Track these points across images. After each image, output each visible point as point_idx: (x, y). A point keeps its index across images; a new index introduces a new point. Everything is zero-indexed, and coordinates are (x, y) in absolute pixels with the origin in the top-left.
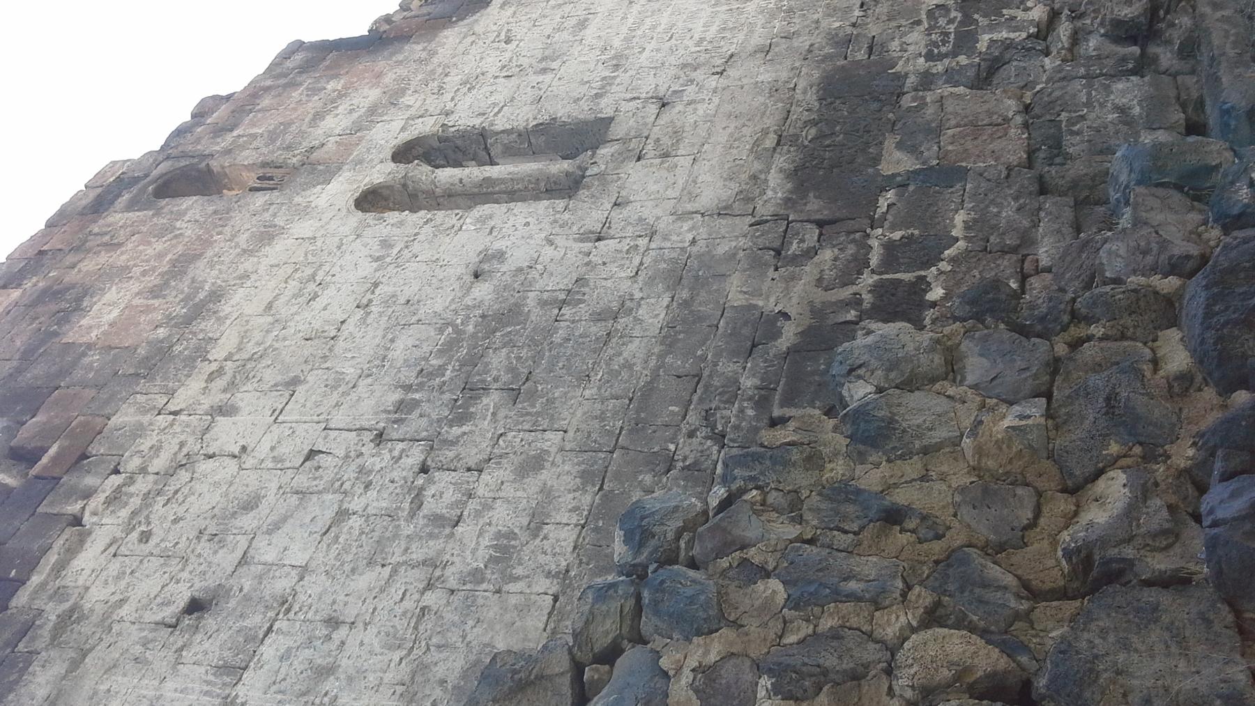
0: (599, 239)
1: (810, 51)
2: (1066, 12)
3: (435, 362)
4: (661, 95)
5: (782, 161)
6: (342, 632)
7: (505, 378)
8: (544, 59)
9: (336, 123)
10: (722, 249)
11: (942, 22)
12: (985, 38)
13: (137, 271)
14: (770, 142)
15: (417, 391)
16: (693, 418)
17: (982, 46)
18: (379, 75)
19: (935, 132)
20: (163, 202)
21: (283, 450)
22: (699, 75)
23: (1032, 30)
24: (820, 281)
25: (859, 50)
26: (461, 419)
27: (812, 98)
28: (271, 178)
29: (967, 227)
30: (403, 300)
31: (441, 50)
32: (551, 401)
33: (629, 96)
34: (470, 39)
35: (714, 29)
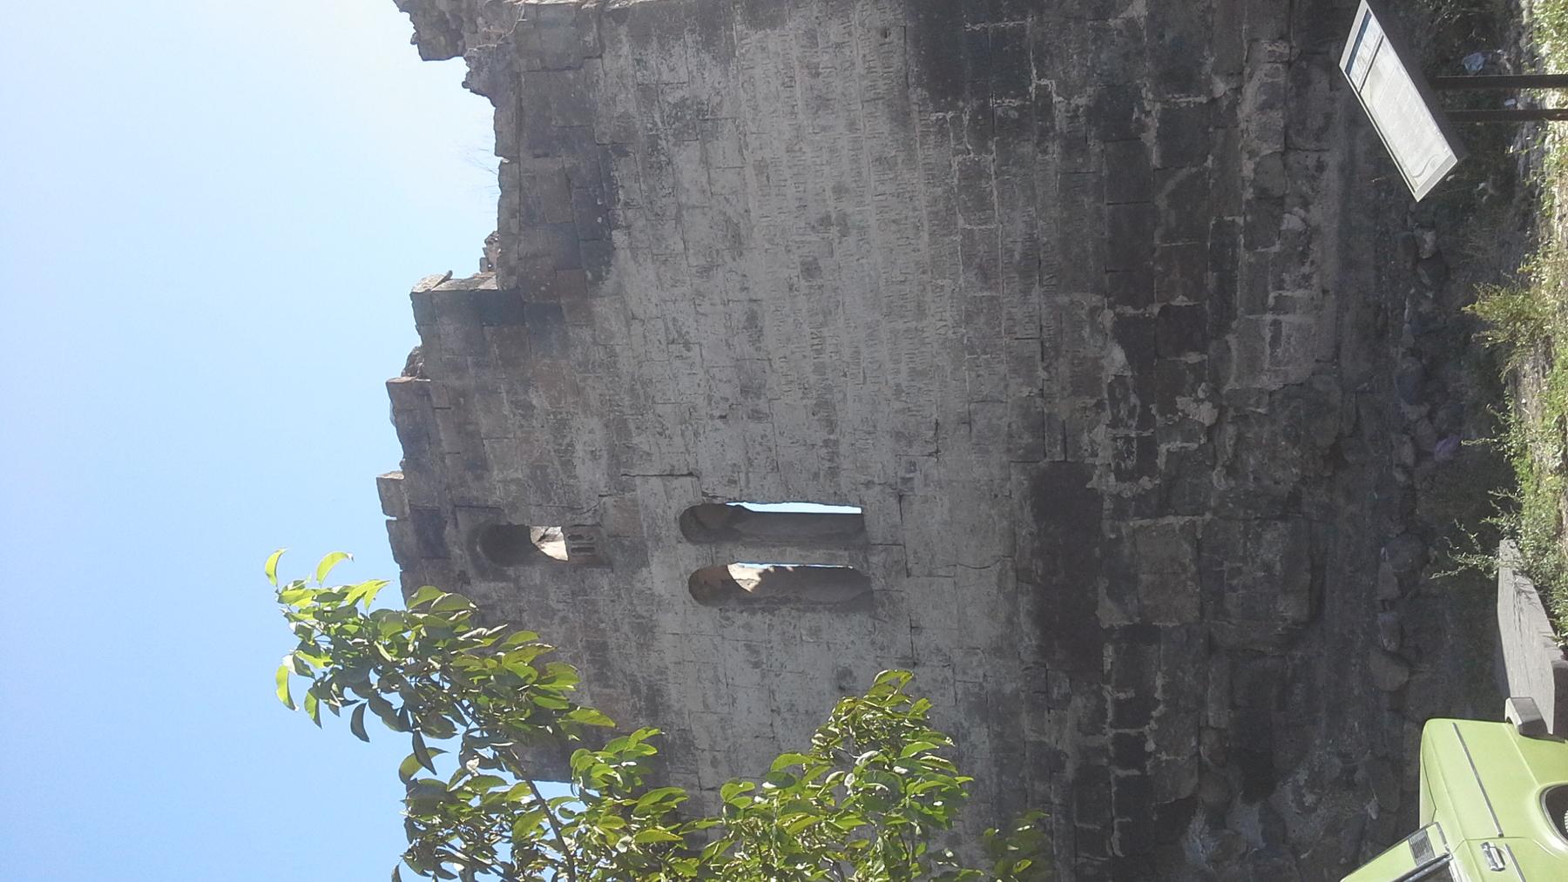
1: (1010, 436)
2: (1231, 412)
4: (892, 481)
5: (1025, 603)
8: (745, 391)
9: (590, 475)
10: (1008, 688)
12: (1163, 448)
17: (1161, 462)
18: (578, 391)
20: (511, 571)
22: (915, 451)
24: (1079, 724)
27: (1027, 514)
28: (580, 537)
29: (1164, 691)
30: (802, 710)
31: (618, 349)
33: (863, 478)
34: (636, 327)
35: (904, 368)
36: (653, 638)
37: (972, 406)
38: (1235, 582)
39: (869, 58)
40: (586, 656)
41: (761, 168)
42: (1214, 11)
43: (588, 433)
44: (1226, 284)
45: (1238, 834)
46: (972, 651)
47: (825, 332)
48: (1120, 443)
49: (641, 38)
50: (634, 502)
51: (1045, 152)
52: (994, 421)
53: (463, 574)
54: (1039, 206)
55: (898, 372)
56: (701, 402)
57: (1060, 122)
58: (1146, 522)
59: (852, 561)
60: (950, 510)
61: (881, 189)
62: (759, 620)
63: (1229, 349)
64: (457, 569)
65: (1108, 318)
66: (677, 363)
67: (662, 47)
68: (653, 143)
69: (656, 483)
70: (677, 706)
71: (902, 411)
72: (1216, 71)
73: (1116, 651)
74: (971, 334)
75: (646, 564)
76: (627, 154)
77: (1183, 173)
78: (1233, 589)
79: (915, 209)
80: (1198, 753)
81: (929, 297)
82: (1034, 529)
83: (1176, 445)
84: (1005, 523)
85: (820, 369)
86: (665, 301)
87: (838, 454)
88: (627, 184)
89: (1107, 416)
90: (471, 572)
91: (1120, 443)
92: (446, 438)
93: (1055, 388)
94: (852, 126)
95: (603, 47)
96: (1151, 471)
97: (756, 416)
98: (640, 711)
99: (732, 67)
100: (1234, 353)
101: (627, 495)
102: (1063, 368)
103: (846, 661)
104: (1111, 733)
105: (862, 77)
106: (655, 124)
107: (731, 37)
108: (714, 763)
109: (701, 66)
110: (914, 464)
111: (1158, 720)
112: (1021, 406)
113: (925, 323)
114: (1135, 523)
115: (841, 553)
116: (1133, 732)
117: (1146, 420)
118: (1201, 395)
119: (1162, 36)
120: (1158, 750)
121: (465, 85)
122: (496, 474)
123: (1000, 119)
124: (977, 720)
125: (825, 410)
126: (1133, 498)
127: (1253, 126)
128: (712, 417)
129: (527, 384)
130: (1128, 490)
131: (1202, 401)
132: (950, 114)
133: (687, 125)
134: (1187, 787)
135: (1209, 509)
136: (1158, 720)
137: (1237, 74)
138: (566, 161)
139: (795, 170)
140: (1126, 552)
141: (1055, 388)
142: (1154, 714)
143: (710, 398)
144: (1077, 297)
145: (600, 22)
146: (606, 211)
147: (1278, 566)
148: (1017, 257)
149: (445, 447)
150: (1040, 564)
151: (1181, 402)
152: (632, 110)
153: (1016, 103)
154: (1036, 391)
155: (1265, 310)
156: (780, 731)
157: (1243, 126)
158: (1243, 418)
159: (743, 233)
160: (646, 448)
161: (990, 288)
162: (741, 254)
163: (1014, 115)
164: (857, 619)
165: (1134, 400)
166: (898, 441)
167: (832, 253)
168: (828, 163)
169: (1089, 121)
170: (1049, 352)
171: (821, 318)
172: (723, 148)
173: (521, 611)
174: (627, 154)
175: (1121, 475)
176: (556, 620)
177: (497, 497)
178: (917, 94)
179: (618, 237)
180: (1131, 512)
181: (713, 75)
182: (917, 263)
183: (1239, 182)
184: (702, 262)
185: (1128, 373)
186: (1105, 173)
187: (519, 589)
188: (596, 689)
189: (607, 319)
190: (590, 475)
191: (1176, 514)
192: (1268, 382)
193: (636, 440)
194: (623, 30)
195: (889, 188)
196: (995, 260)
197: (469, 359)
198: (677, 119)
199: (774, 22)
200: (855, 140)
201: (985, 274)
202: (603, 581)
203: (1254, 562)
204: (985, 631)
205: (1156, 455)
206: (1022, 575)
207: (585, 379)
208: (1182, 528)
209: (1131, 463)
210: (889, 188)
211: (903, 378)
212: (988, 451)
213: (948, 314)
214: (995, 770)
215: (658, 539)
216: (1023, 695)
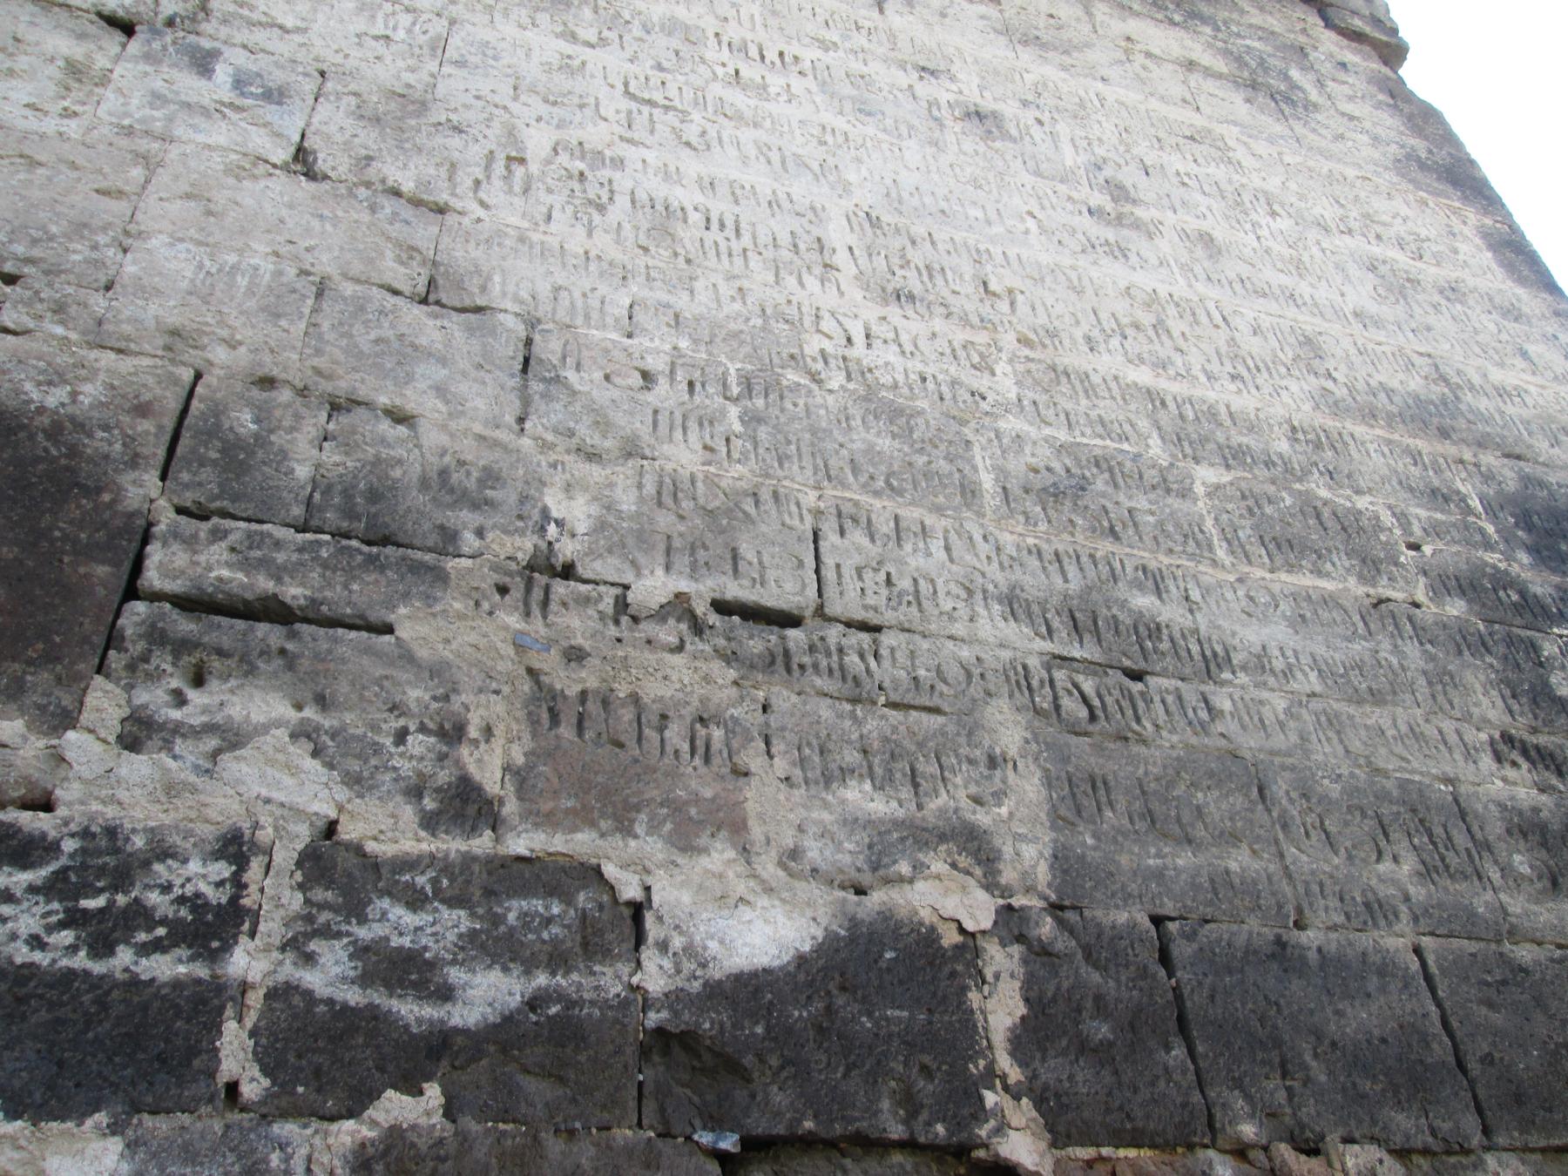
4: (205, 27)
11: (437, 928)
25: (246, 565)
65: (945, 899)
89: (387, 828)
91: (203, 876)
93: (578, 625)
102: (679, 676)
113: (858, 295)
117: (327, 1057)
123: (1534, 647)
144: (1028, 788)
148: (1143, 601)
154: (567, 549)
159: (1050, 55)
165: (486, 994)
167: (1038, 173)
185: (655, 975)
201: (1060, 493)
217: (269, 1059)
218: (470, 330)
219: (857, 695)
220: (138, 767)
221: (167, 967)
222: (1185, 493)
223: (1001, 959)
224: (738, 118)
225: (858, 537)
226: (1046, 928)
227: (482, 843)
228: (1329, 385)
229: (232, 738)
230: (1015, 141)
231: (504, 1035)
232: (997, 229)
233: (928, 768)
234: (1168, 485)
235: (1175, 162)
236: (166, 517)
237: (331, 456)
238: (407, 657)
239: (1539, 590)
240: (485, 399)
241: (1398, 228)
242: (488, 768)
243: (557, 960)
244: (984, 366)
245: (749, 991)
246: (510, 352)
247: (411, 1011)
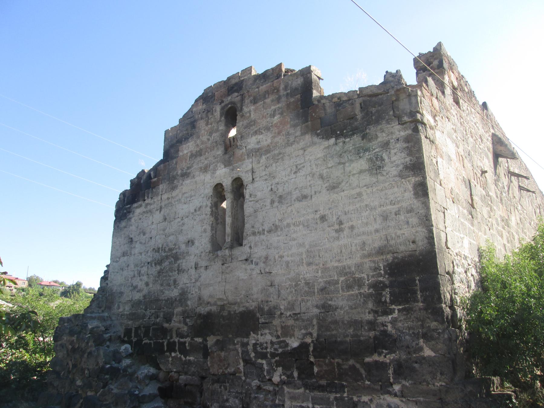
0: (196, 268)
1: (267, 302)
2: (277, 389)
3: (167, 249)
5: (214, 308)
6: (126, 268)
7: (163, 268)
8: (281, 197)
9: (252, 142)
10: (189, 303)
12: (264, 362)
13: (198, 142)
14: (219, 303)
15: (162, 250)
16: (153, 311)
17: (260, 361)
18: (279, 133)
19: (222, 349)
20: (223, 118)
21: (153, 231)
22: (262, 265)
23: (267, 377)
24: (179, 328)
26: (156, 264)
27: (241, 309)
28: (234, 141)
29: (189, 360)
30: (183, 228)
31: (294, 146)
32: (158, 281)
33: (252, 245)
34: (301, 152)
35: (289, 259)
36: (203, 172)
37: (277, 286)
38: (222, 387)
39: (403, 236)
40: (198, 149)
41: (360, 194)
42: (428, 386)
43: (265, 139)
44: (321, 388)
45: (147, 385)
46: (200, 289)
47: (301, 226)
48: (265, 345)
49: (407, 140)
50: (244, 159)
51: (369, 313)
52: (272, 295)
53: (222, 102)
54: (349, 311)
55: (288, 256)
56: (277, 180)
57: (381, 319)
58: (240, 354)
59: (228, 242)
60: (243, 279)
61: (353, 245)
62: (209, 209)
63: (299, 389)
64: (224, 100)
65: (308, 340)
66: (289, 169)
67: (404, 149)
68: (367, 150)
69: (250, 167)
70: (184, 183)
71: (275, 259)
72: (403, 386)
73: (200, 343)
74: (302, 285)
75: (225, 166)
76: (363, 140)
77: (363, 371)
78: (220, 387)
79: (346, 259)
80: (172, 372)
81: (314, 267)
82: (237, 312)
83: (266, 367)
84: (239, 300)
85: (288, 225)
86: (310, 162)
87: (260, 235)
88: (352, 141)
89: (274, 340)
90: (223, 105)
91: (265, 345)
92: (264, 88)
94: (377, 231)
95: (403, 124)
96: (257, 357)
97: (272, 202)
98: (183, 171)
99: (397, 179)
100: (297, 391)
101: (246, 157)
102: (291, 322)
103: (197, 243)
104: (176, 340)
105: (396, 234)
106: (374, 149)
107: (409, 177)
108: (168, 198)
109: (397, 166)
110: (257, 264)
111: (180, 357)
112: (277, 306)
113: (305, 266)
114: (240, 351)
115: (230, 238)
116: (177, 348)
118: (283, 377)
119: (416, 363)
120: (172, 357)
121: (387, 72)
122: (252, 108)
123: (382, 293)
124: (180, 292)
125: (275, 229)
126: (248, 350)
127: (382, 401)
128: (272, 185)
129: (281, 114)
130: (250, 348)
131: (280, 378)
132: (382, 272)
133: (374, 163)
134: (162, 366)
135: (246, 379)
136: (180, 357)
137: (402, 395)
138: (359, 116)
139: (359, 209)
140: (231, 347)
141: (283, 319)
142: (182, 356)
143: (278, 184)
144: (316, 328)
145: (411, 122)
146: (342, 135)
147: (228, 404)
148: (330, 302)
149: (261, 88)
150: (226, 314)
151: (280, 369)
152: (379, 139)
153: (388, 300)
154: (283, 311)
155: (313, 404)
156: (177, 221)
157: (382, 397)
158: (275, 393)
159: (336, 190)
160: (261, 161)
161: (318, 292)
162: (328, 190)
163: (383, 299)
164: (209, 247)
165: (280, 350)
166: (265, 258)
167: (329, 227)
168: (362, 222)
169: (382, 331)
170: (296, 316)
171: (306, 224)
172: (367, 179)
173: (211, 124)
174: (363, 140)
175: (255, 345)
176: (209, 137)
177: (245, 109)
178: (390, 257)
179: (332, 141)
180: (243, 349)
181: (394, 171)
182: (326, 262)
183: (360, 395)
184: (325, 175)
185: (289, 348)
186: (362, 338)
187: (218, 123)
188: (189, 154)
189: (304, 140)
190: (252, 142)
191: (244, 366)
192: (288, 403)
193: (264, 157)
194: (410, 132)
195: (354, 248)
196: (328, 294)
197: (289, 91)
198: (377, 158)
199: (416, 194)
200: (371, 233)
201: (323, 290)
202: (220, 152)
203: (229, 395)
204: (206, 293)
205: (262, 359)
206: (222, 307)
207: (283, 135)
208: (239, 368)
209: (259, 349)
210: (354, 248)
211: (286, 259)
212: (262, 293)
213: (308, 275)
214: (166, 298)
215: (233, 170)
216: (187, 308)
217: (270, 356)
218: (275, 288)
219: (303, 321)
220: (262, 337)
221: (265, 351)
222: (338, 283)
223: (312, 345)
224: (294, 240)
225: (304, 303)
226: (315, 342)
227: (279, 340)
228: (364, 252)
229: (266, 334)
230: (326, 220)
231: (281, 353)
232: (322, 244)
233: (308, 327)
234: (337, 282)
235: (351, 208)
236: (260, 316)
237: (267, 308)
238: (274, 325)
239: (386, 282)
240: (275, 297)
241: (392, 197)
242: (279, 333)
243: (284, 348)
244: (318, 272)
245: (295, 349)
246: (277, 289)
247: (277, 352)
